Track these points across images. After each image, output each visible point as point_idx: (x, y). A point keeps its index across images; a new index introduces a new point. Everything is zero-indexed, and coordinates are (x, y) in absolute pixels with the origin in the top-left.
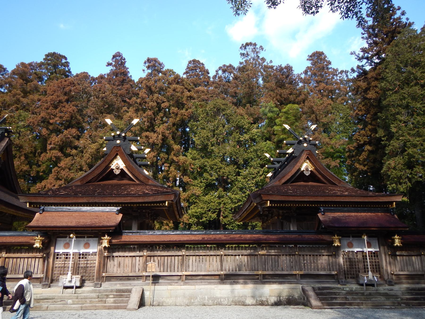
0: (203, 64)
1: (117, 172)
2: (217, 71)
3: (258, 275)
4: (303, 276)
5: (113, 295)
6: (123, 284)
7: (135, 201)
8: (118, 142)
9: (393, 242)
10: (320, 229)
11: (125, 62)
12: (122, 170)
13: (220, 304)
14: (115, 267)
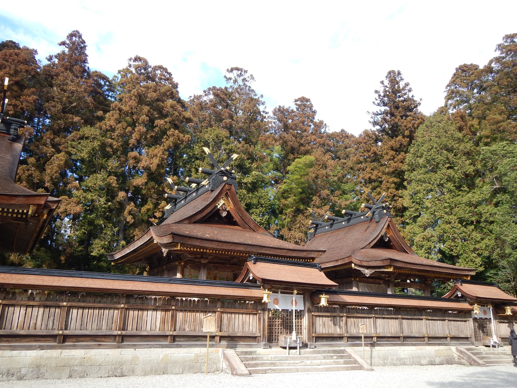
0: (170, 74)
1: (224, 214)
2: (205, 92)
3: (424, 337)
4: (453, 338)
5: (337, 356)
6: (330, 344)
7: (290, 255)
8: (225, 178)
9: (504, 311)
10: (452, 298)
11: (85, 47)
12: (228, 212)
13: (404, 364)
14: (321, 327)
